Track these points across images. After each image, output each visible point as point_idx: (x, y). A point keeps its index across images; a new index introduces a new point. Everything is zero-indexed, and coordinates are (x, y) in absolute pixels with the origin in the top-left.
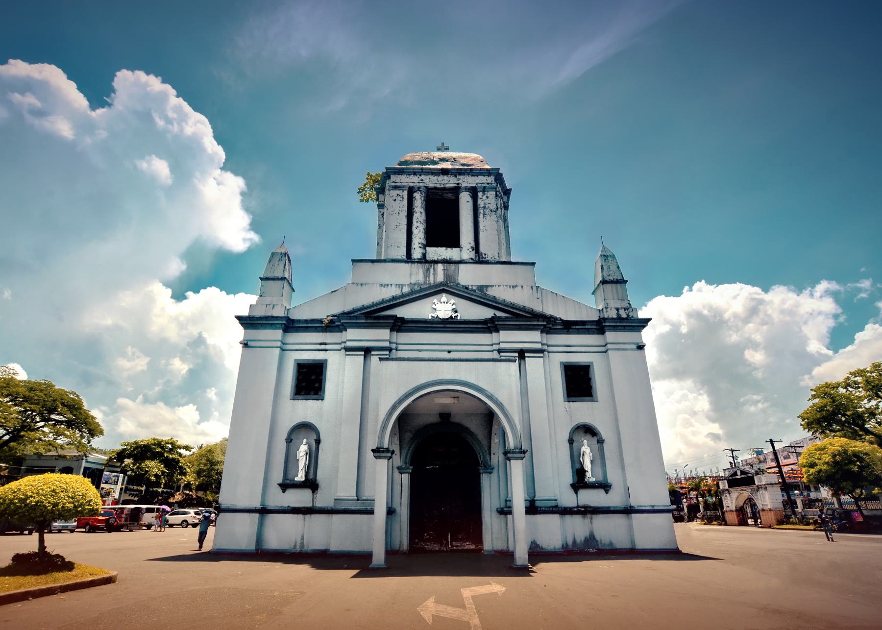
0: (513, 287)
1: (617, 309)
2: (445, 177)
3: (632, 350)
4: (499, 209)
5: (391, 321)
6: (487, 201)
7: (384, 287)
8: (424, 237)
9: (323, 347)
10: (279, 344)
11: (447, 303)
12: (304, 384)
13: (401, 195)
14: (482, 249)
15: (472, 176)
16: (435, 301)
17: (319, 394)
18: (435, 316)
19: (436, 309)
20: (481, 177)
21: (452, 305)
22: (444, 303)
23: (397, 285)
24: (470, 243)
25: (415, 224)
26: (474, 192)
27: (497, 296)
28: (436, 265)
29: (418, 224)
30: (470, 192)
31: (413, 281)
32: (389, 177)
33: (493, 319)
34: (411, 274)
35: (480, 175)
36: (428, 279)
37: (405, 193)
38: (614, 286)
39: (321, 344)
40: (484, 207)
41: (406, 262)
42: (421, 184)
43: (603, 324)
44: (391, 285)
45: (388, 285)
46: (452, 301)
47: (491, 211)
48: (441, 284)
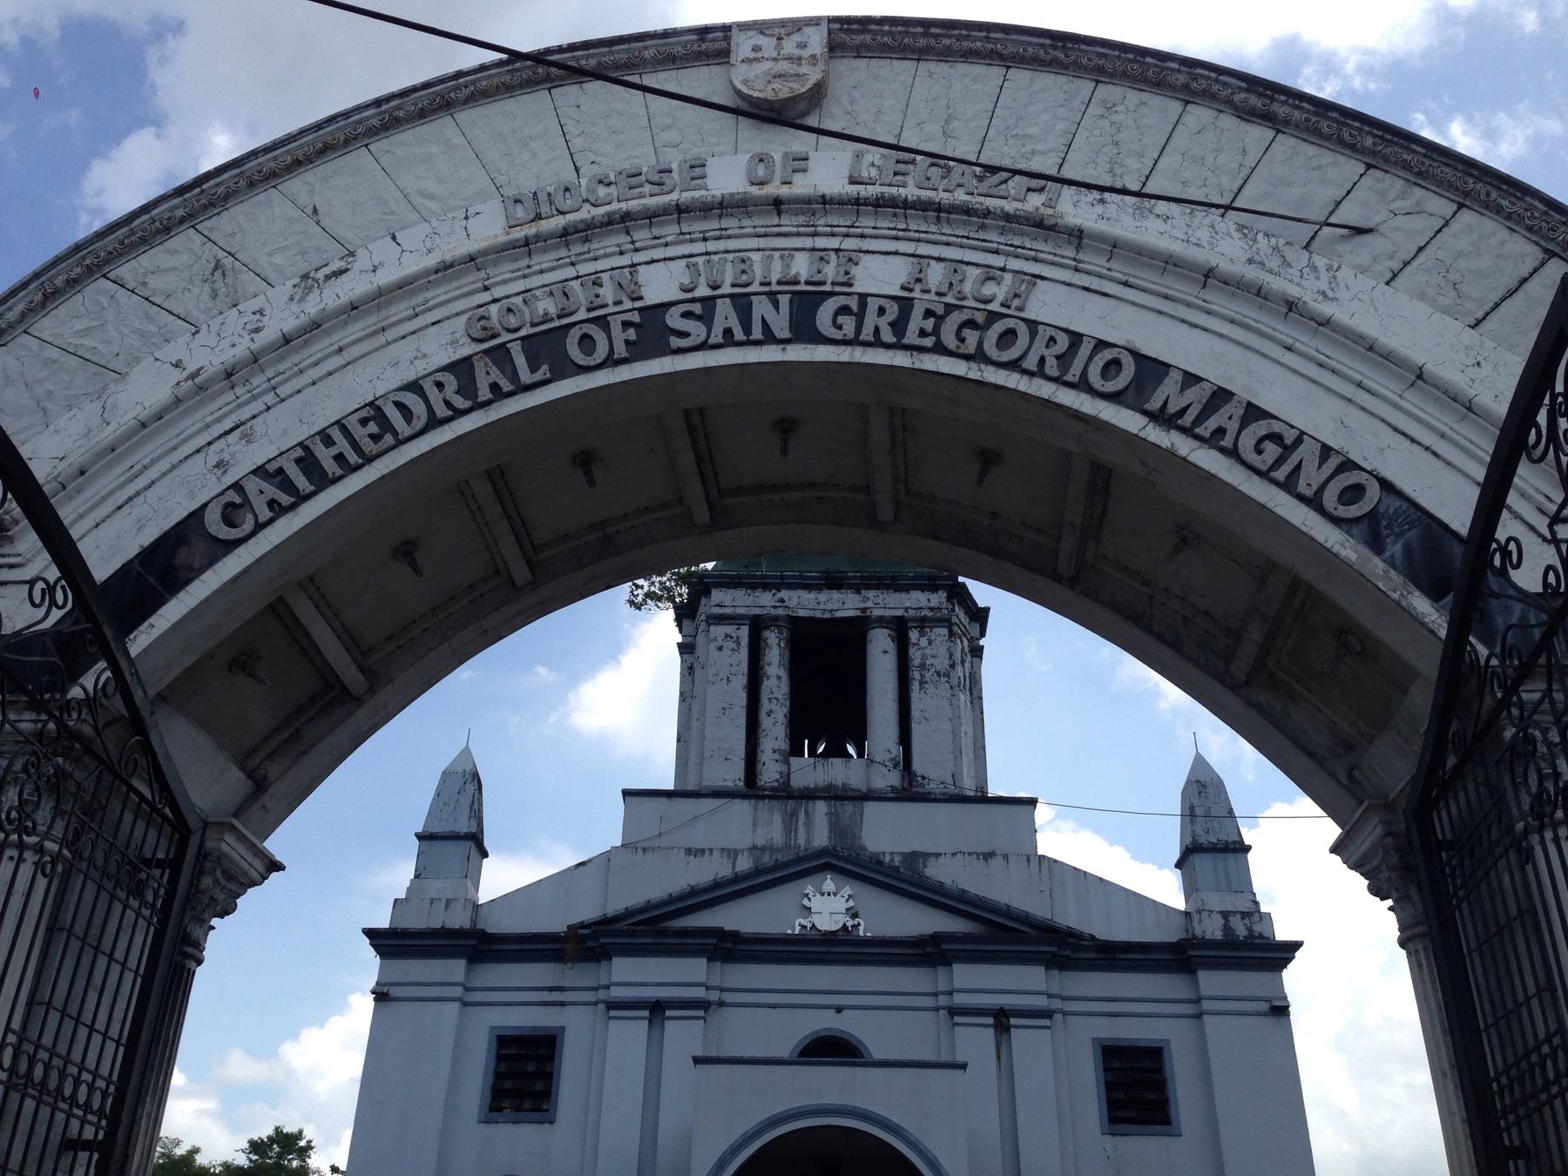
0: (988, 856)
3: (1259, 1014)
4: (959, 668)
5: (710, 941)
6: (928, 651)
7: (695, 856)
8: (786, 735)
9: (555, 996)
10: (458, 992)
11: (835, 895)
12: (508, 1084)
13: (734, 635)
14: (917, 766)
15: (896, 591)
16: (809, 890)
17: (544, 1107)
18: (809, 925)
19: (810, 909)
21: (847, 901)
22: (829, 894)
23: (723, 850)
24: (889, 751)
25: (765, 705)
26: (900, 628)
27: (947, 881)
28: (811, 804)
29: (773, 706)
30: (891, 629)
31: (760, 842)
32: (708, 593)
33: (936, 938)
34: (755, 824)
36: (793, 837)
37: (744, 632)
38: (1219, 856)
39: (551, 989)
40: (923, 666)
41: (743, 796)
42: (780, 612)
44: (711, 850)
45: (702, 852)
46: (847, 891)
47: (938, 674)
48: (824, 852)
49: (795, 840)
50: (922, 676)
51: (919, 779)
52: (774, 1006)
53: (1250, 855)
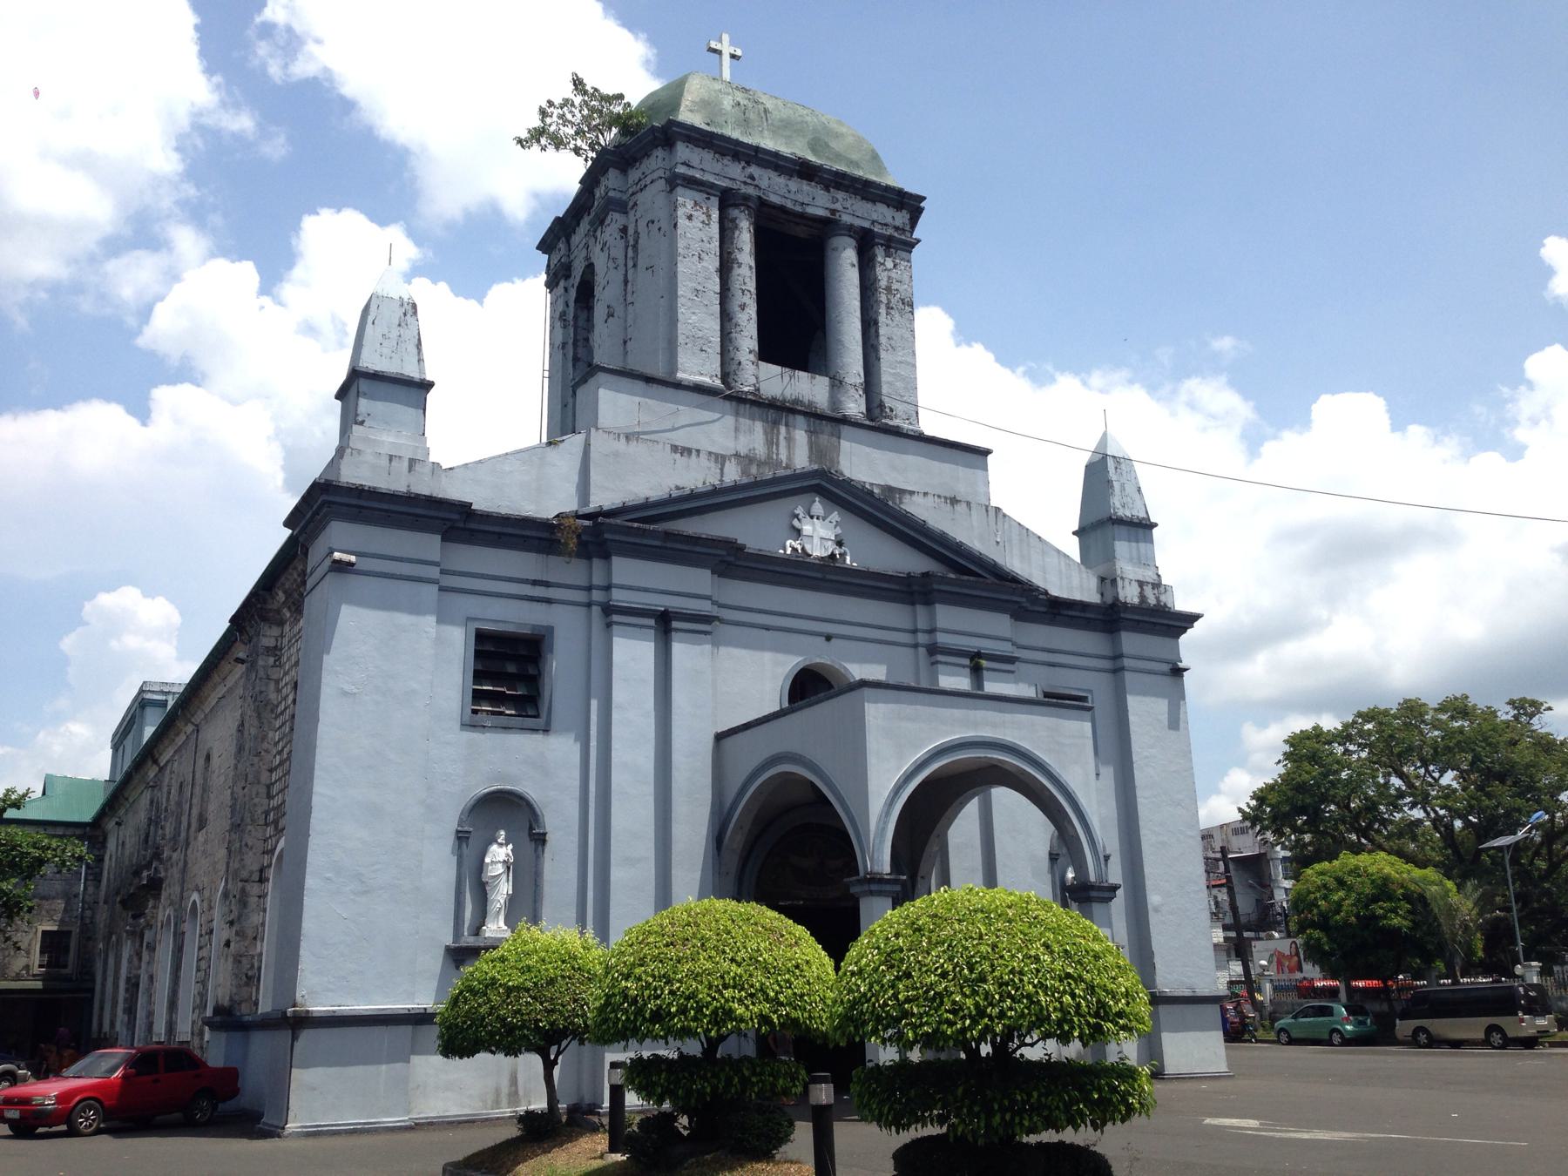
1: (1141, 584)
2: (806, 186)
3: (1164, 674)
6: (893, 274)
15: (863, 199)
20: (881, 208)
23: (710, 453)
26: (866, 243)
35: (880, 202)
36: (774, 449)
39: (535, 583)
42: (751, 191)
43: (1122, 615)
45: (689, 451)
46: (835, 516)
49: (777, 454)
50: (889, 301)
51: (888, 410)
52: (768, 628)
53: (1155, 531)
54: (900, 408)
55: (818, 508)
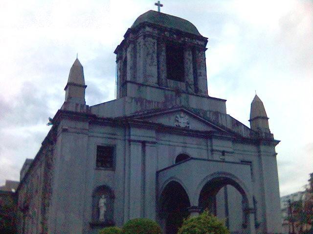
9: (112, 136)
54: (203, 90)
55: (182, 115)
